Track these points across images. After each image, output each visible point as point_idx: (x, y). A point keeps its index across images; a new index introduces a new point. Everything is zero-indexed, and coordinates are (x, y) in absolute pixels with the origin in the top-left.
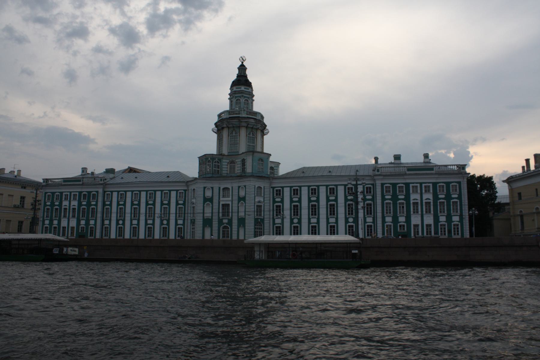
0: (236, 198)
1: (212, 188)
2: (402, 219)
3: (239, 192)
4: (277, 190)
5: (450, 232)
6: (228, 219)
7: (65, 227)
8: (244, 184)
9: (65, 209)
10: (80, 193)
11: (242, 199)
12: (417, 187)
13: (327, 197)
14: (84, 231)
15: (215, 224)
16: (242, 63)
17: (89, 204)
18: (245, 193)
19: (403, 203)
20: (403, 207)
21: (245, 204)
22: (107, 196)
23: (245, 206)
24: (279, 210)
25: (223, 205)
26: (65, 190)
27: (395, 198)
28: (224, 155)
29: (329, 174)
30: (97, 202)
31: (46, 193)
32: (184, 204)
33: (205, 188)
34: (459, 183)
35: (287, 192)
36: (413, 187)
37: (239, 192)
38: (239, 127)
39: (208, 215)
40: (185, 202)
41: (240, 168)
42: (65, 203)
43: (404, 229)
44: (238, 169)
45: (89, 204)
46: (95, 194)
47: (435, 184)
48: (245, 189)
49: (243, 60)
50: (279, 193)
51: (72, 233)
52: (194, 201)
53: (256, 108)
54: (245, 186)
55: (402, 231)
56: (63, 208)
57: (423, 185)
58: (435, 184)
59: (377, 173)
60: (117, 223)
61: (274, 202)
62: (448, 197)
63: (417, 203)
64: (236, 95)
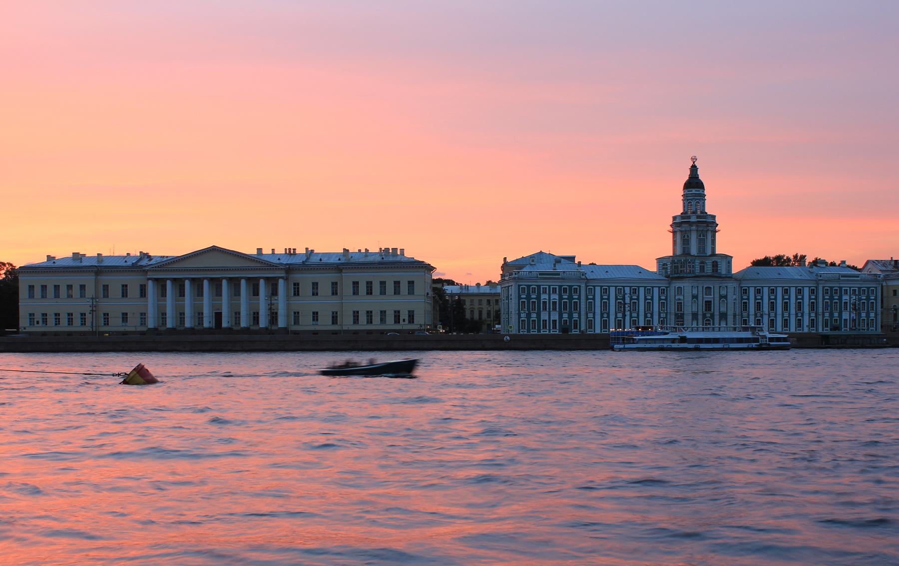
0: (717, 296)
1: (698, 287)
2: (836, 315)
3: (720, 291)
4: (744, 289)
5: (868, 325)
6: (711, 313)
7: (546, 321)
8: (726, 285)
9: (545, 303)
10: (560, 287)
11: (724, 297)
12: (847, 290)
13: (783, 296)
14: (567, 323)
15: (700, 317)
16: (694, 163)
17: (570, 298)
18: (727, 292)
19: (837, 303)
20: (837, 305)
21: (727, 300)
22: (591, 291)
23: (727, 304)
24: (745, 306)
25: (706, 301)
26: (544, 284)
27: (832, 298)
28: (694, 256)
29: (778, 277)
30: (580, 296)
31: (519, 286)
32: (666, 299)
33: (692, 286)
34: (876, 288)
35: (752, 291)
36: (844, 290)
37: (720, 291)
38: (707, 231)
39: (695, 309)
40: (666, 297)
41: (710, 269)
42: (544, 297)
43: (837, 322)
44: (709, 269)
45: (570, 298)
46: (577, 289)
47: (859, 288)
48: (727, 289)
49: (694, 159)
50: (745, 291)
51: (554, 327)
52: (682, 297)
53: (709, 210)
54: (727, 287)
55: (836, 324)
56: (542, 302)
57: (852, 288)
58: (859, 288)
59: (819, 278)
60: (602, 316)
61: (742, 299)
62: (868, 299)
63: (847, 302)
64: (696, 198)
